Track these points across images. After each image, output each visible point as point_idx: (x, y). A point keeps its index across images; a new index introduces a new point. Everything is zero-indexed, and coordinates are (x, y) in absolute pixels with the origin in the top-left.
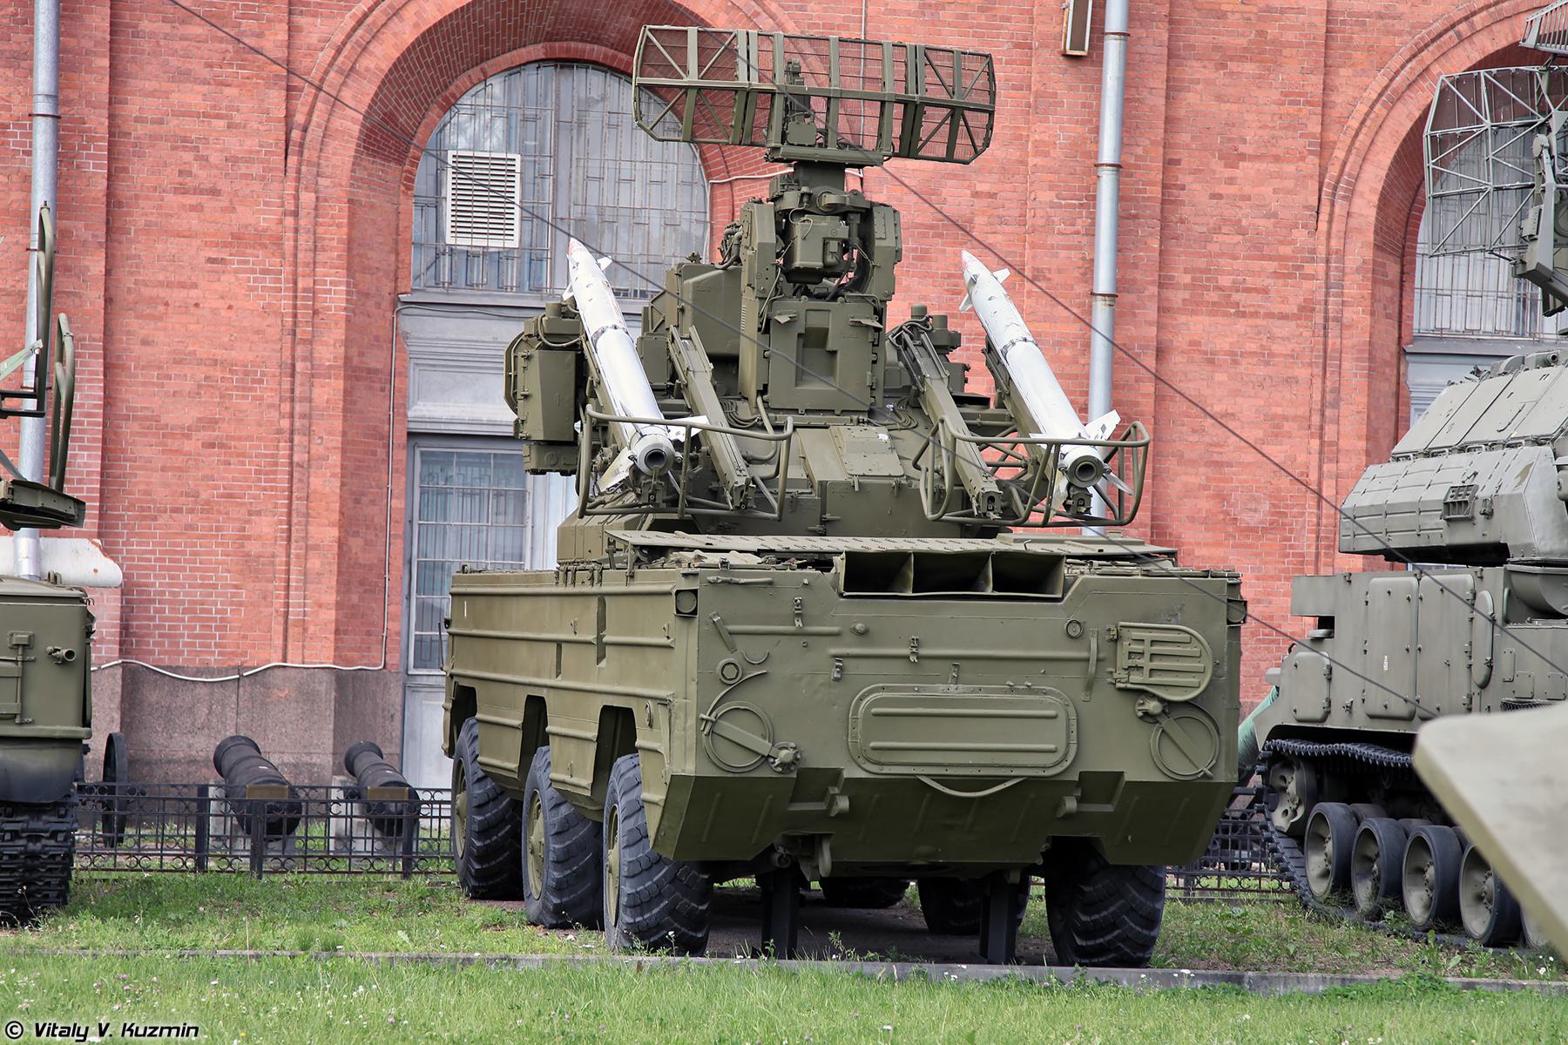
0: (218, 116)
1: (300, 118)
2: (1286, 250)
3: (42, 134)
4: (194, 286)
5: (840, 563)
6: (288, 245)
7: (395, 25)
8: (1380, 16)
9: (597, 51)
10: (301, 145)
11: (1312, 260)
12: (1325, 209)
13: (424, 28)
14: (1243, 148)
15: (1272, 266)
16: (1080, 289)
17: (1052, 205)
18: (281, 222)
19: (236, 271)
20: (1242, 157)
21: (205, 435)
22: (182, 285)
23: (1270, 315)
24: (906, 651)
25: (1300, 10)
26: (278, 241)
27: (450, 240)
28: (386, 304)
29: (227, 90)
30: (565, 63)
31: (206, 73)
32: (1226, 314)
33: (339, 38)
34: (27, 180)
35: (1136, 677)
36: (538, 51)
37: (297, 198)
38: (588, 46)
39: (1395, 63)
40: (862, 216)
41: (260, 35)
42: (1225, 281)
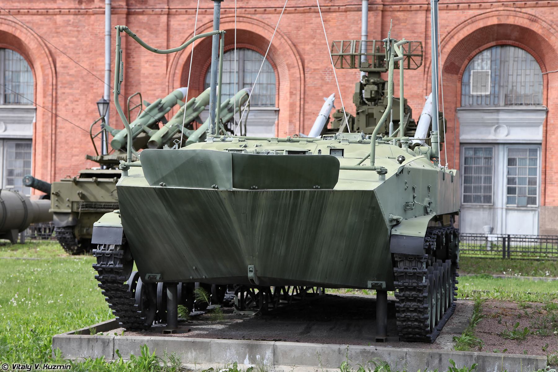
7: (452, 40)
9: (510, 42)
10: (428, 72)
13: (459, 40)
27: (471, 93)
28: (453, 110)
30: (503, 46)
37: (427, 85)
38: (507, 41)
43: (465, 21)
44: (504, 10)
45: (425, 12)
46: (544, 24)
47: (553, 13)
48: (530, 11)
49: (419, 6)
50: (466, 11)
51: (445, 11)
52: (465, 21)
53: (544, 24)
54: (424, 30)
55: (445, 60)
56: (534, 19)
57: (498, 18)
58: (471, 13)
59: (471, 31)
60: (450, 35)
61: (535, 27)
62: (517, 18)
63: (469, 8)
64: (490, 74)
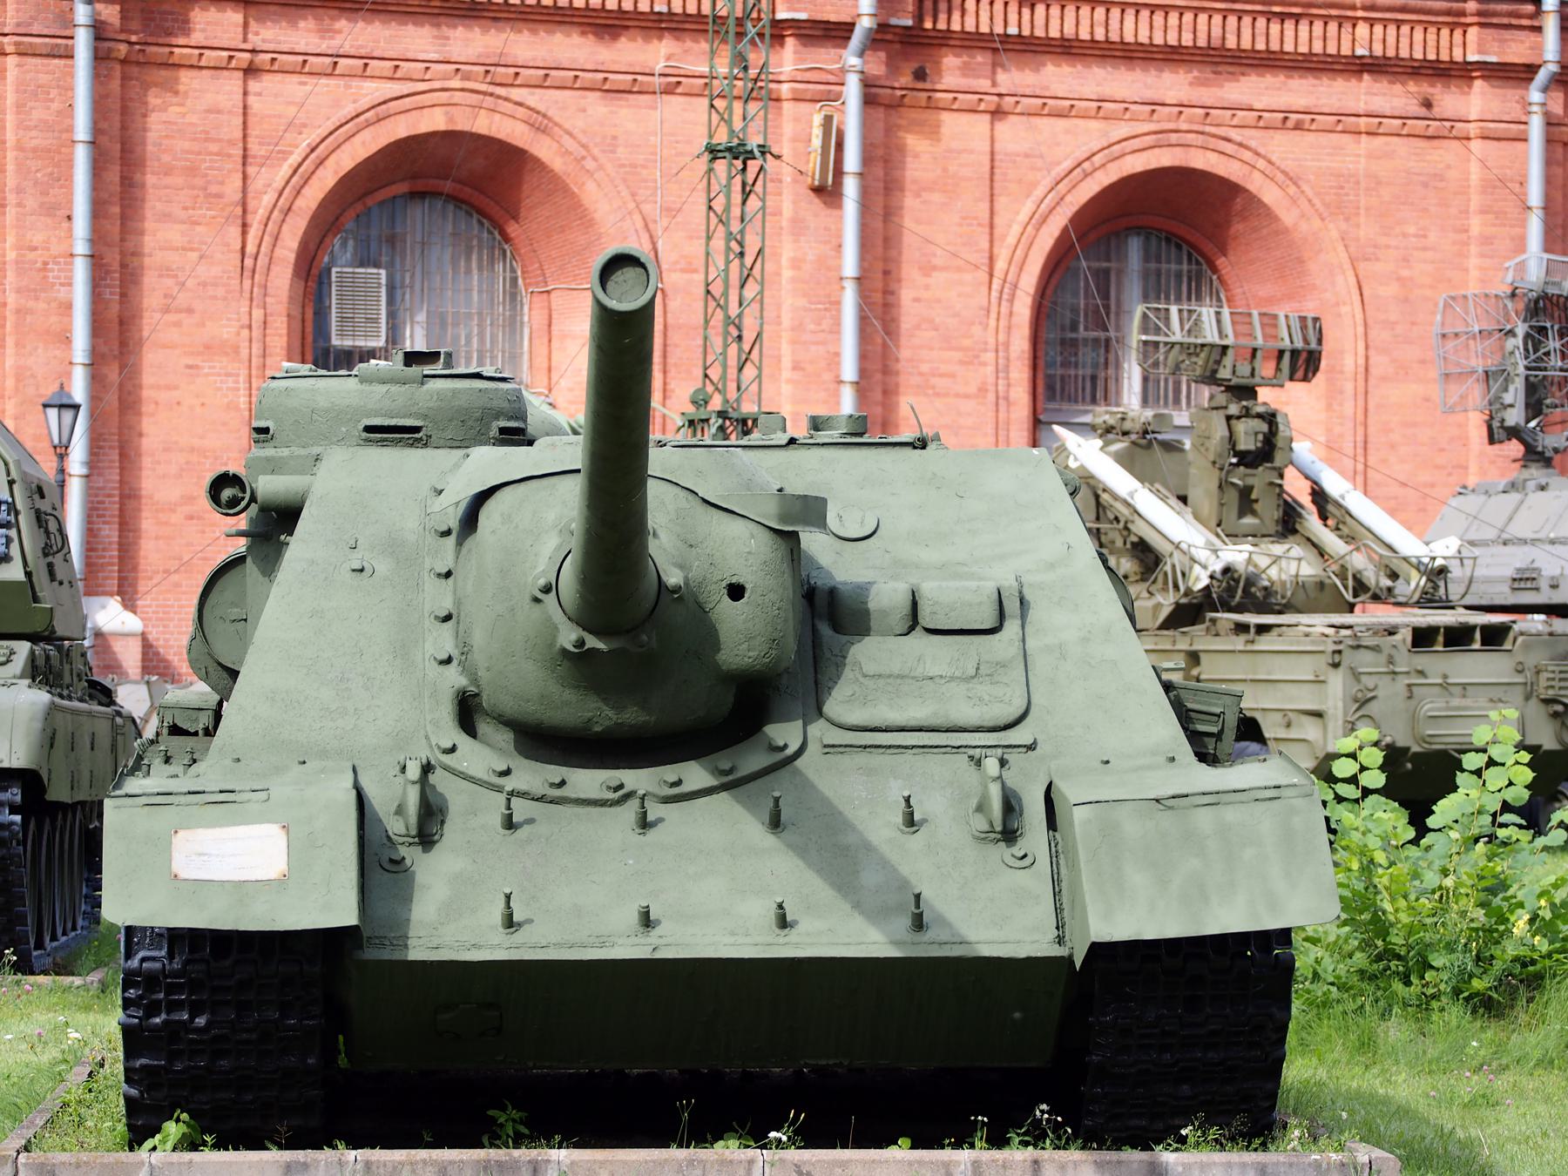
0: (192, 250)
1: (251, 248)
2: (967, 342)
3: (80, 272)
4: (176, 388)
5: (1405, 635)
6: (244, 352)
8: (1027, 156)
9: (448, 186)
11: (986, 350)
12: (994, 309)
14: (938, 261)
15: (957, 355)
16: (827, 376)
17: (806, 310)
18: (238, 334)
19: (207, 375)
20: (934, 268)
21: (187, 509)
22: (169, 388)
23: (957, 395)
24: (1439, 681)
25: (972, 152)
26: (236, 350)
29: (199, 229)
31: (183, 214)
32: (926, 395)
33: (279, 181)
34: (68, 307)
35: (1551, 692)
36: (402, 188)
39: (1039, 192)
40: (1270, 418)
41: (222, 183)
42: (925, 368)
43: (358, 116)
44: (462, 90)
45: (241, 74)
46: (568, 142)
47: (584, 110)
48: (533, 98)
49: (225, 54)
50: (355, 83)
51: (295, 78)
52: (358, 116)
53: (568, 142)
54: (239, 134)
55: (300, 233)
56: (541, 124)
57: (447, 113)
58: (373, 90)
59: (374, 148)
60: (317, 155)
61: (543, 149)
62: (497, 117)
63: (363, 74)
64: (383, 281)
